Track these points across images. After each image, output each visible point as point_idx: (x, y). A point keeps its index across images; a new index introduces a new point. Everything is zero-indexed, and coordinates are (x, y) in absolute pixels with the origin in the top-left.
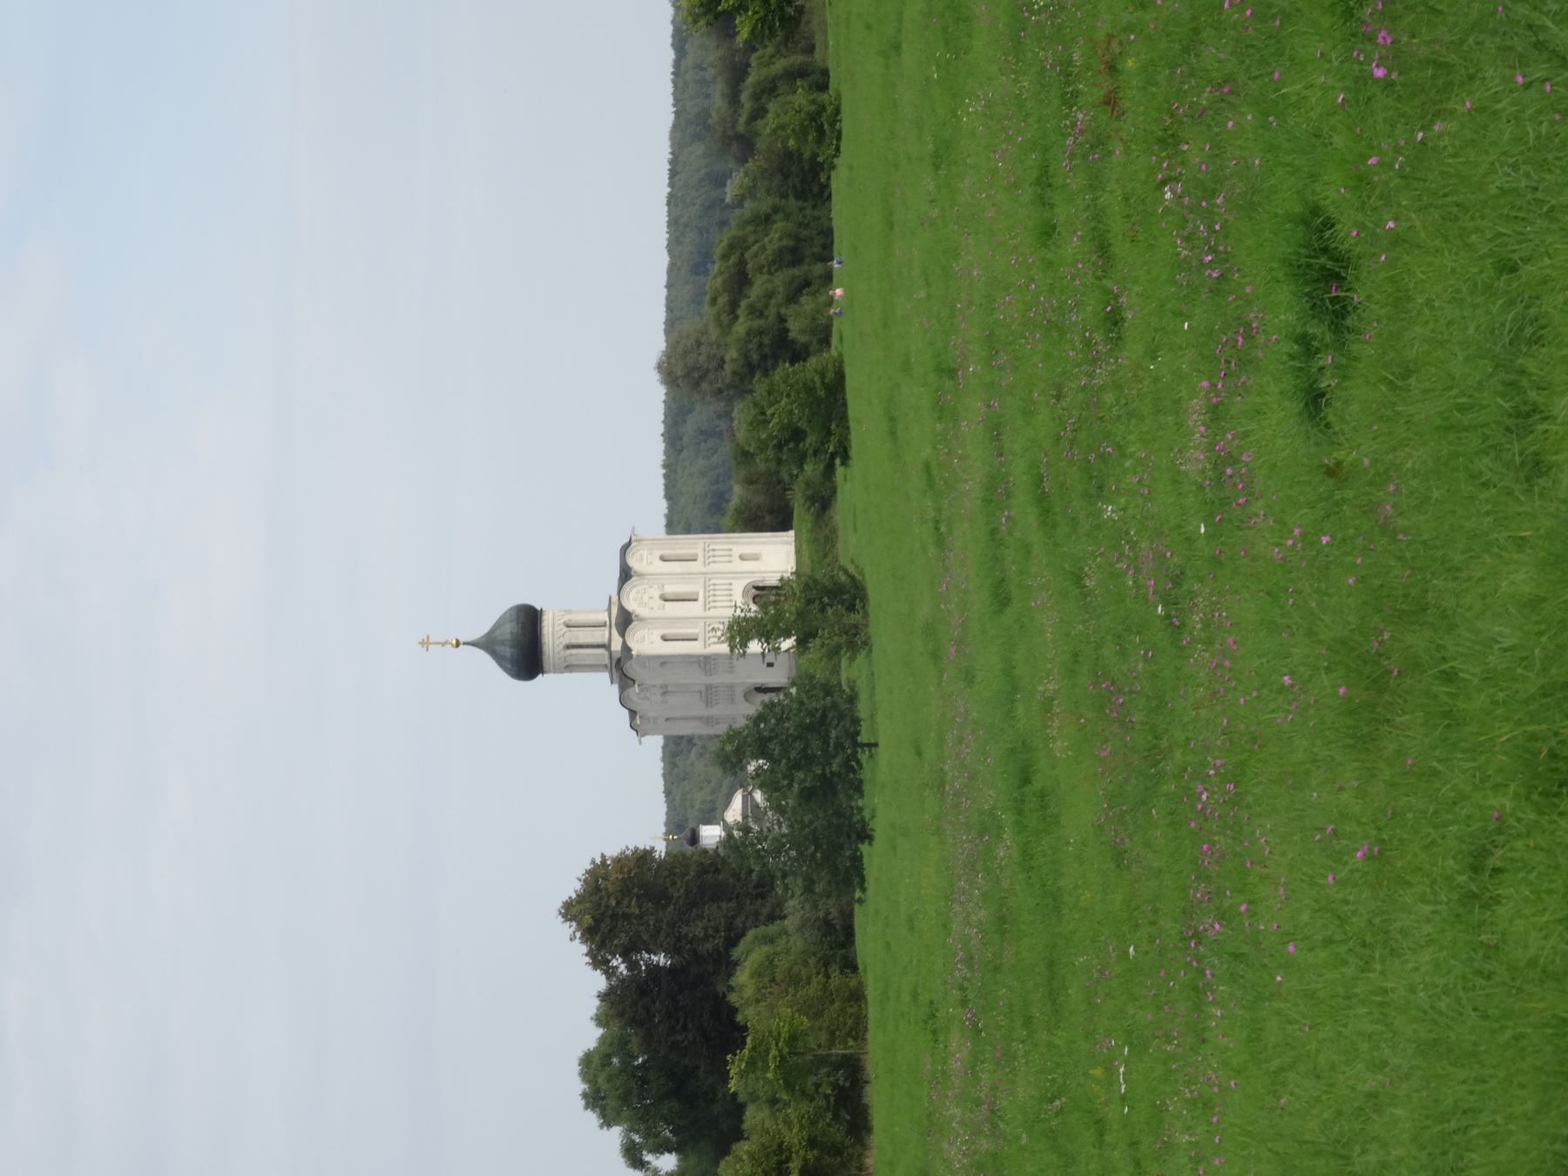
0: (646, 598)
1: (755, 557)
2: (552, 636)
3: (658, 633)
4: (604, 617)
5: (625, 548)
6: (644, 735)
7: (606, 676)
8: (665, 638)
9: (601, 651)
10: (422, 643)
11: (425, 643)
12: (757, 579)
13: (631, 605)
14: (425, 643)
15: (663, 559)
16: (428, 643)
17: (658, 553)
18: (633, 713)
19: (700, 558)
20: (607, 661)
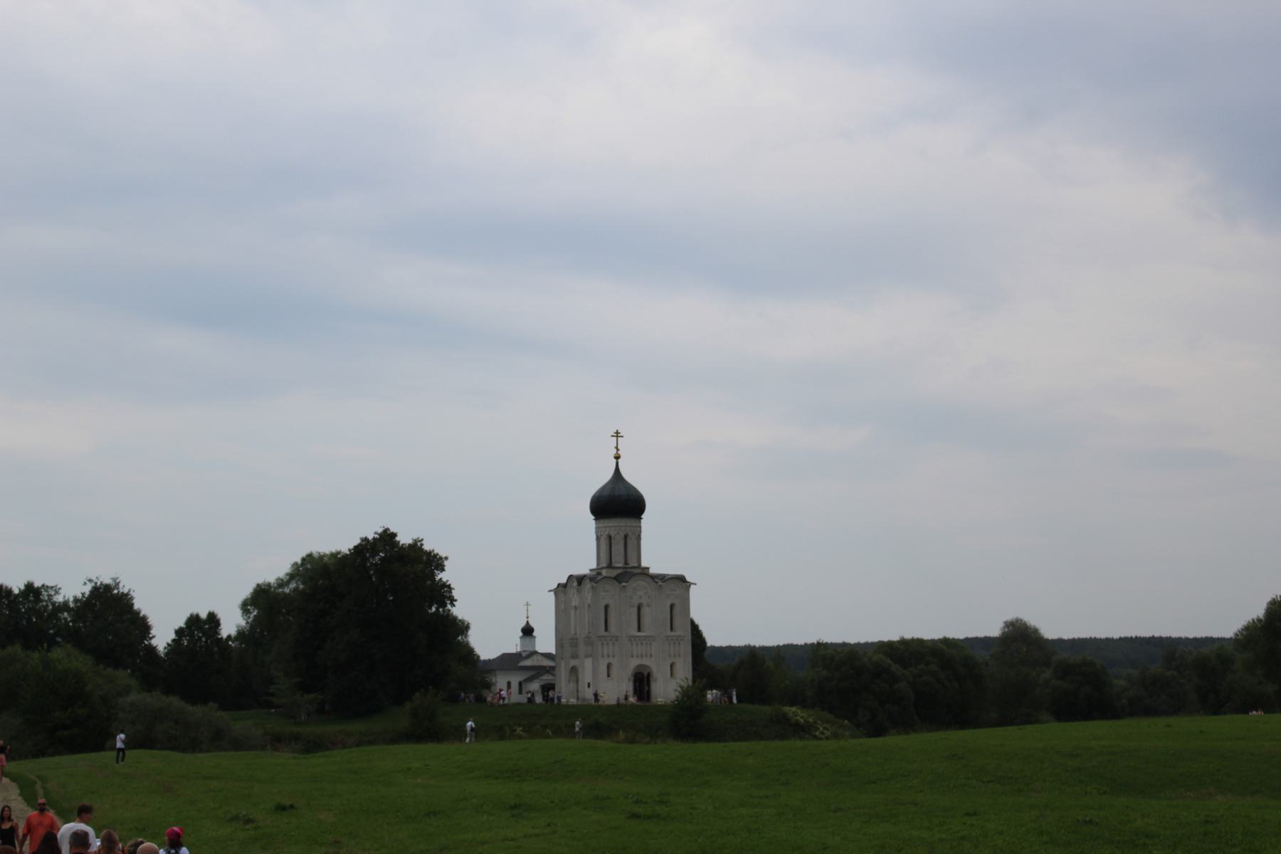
4: (633, 563)
5: (681, 579)
7: (594, 566)
8: (606, 607)
10: (617, 433)
11: (617, 435)
14: (617, 435)
15: (672, 606)
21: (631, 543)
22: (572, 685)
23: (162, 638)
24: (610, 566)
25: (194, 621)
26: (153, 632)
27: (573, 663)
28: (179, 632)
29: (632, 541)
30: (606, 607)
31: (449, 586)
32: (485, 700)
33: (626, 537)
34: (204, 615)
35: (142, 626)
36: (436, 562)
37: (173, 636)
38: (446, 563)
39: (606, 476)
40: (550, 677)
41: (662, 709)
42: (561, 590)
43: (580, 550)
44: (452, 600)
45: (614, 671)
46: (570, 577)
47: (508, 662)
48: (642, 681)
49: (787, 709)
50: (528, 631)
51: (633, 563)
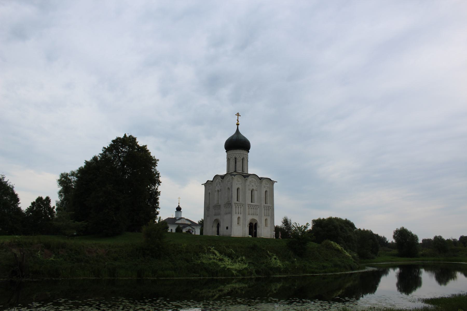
0: (252, 184)
1: (266, 225)
3: (240, 187)
6: (205, 186)
8: (238, 189)
9: (234, 170)
10: (238, 114)
12: (259, 224)
13: (250, 179)
14: (238, 115)
15: (266, 191)
16: (238, 116)
17: (268, 190)
18: (212, 181)
19: (266, 205)
20: (230, 172)
22: (215, 229)
23: (25, 204)
24: (235, 171)
25: (40, 199)
26: (20, 202)
27: (215, 218)
28: (33, 204)
29: (244, 161)
31: (159, 174)
32: (182, 231)
33: (243, 159)
34: (44, 198)
35: (15, 199)
37: (30, 205)
38: (157, 162)
39: (232, 132)
40: (190, 228)
42: (208, 184)
44: (159, 182)
46: (216, 176)
47: (171, 221)
48: (253, 227)
49: (332, 242)
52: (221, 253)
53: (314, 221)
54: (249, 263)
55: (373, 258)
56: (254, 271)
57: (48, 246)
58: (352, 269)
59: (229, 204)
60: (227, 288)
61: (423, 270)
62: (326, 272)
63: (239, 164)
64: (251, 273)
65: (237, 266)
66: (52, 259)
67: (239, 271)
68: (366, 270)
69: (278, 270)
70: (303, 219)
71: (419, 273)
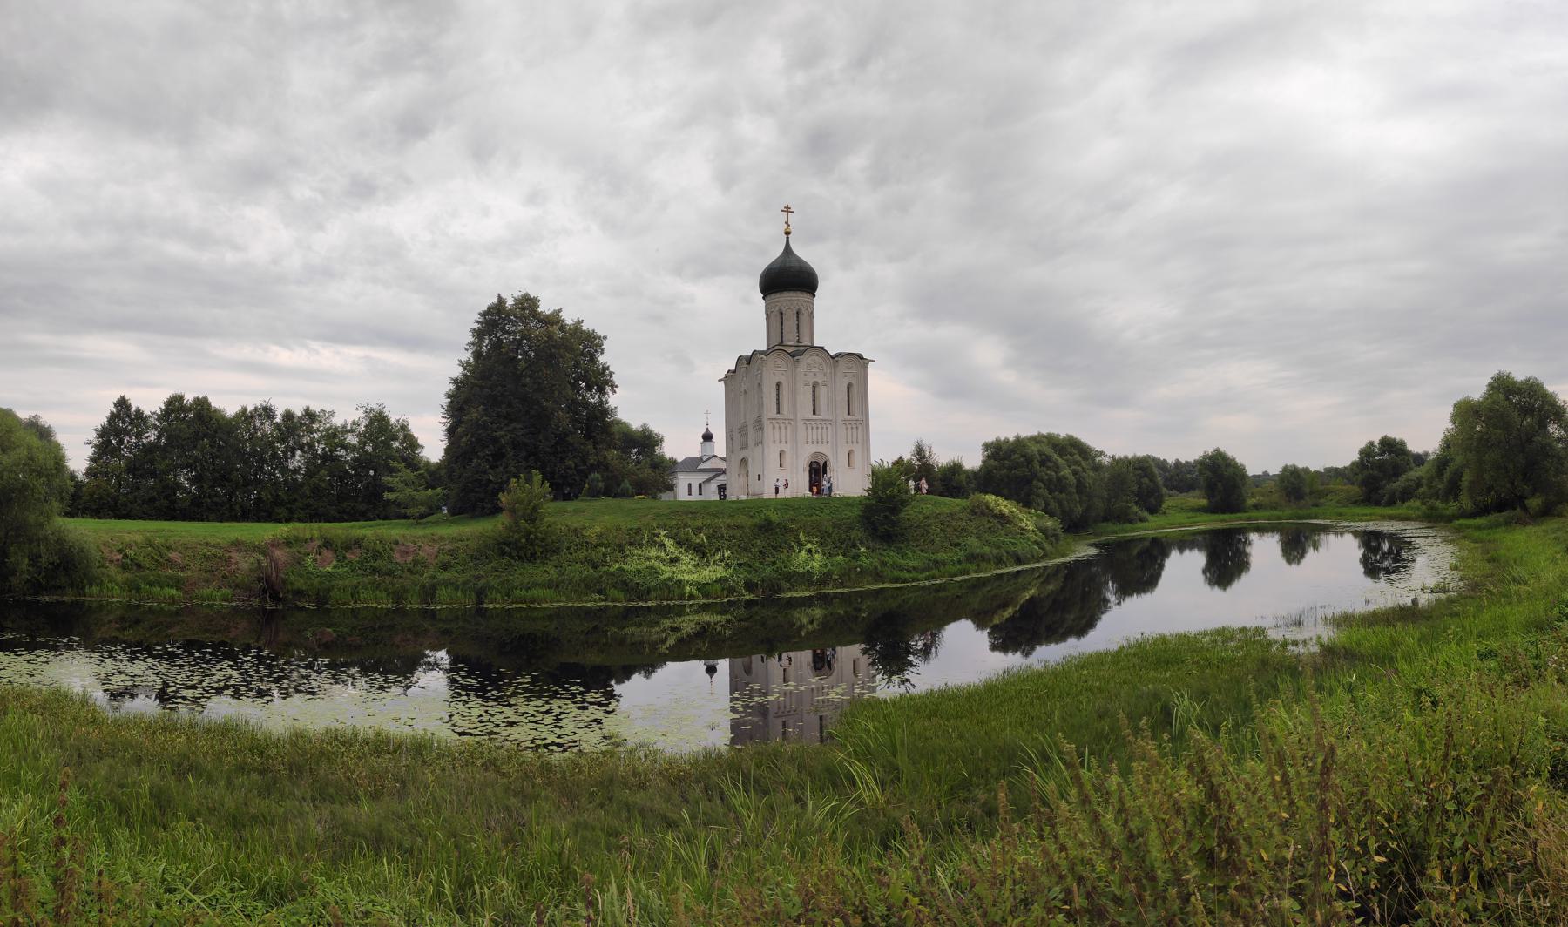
2: (789, 300)
3: (783, 379)
4: (805, 342)
5: (860, 357)
8: (778, 385)
11: (787, 210)
13: (806, 360)
14: (787, 210)
21: (804, 318)
27: (743, 454)
29: (804, 318)
30: (778, 385)
36: (587, 343)
41: (847, 502)
42: (730, 378)
43: (746, 321)
45: (787, 460)
48: (817, 471)
49: (990, 498)
50: (708, 437)
51: (805, 342)
52: (679, 543)
53: (987, 446)
54: (740, 565)
55: (1142, 520)
56: (741, 583)
57: (327, 544)
58: (1019, 561)
59: (759, 421)
60: (688, 623)
61: (1253, 537)
62: (934, 578)
63: (790, 324)
64: (731, 591)
65: (710, 573)
66: (329, 569)
67: (702, 587)
68: (1070, 558)
69: (806, 578)
70: (962, 445)
71: (1247, 542)
